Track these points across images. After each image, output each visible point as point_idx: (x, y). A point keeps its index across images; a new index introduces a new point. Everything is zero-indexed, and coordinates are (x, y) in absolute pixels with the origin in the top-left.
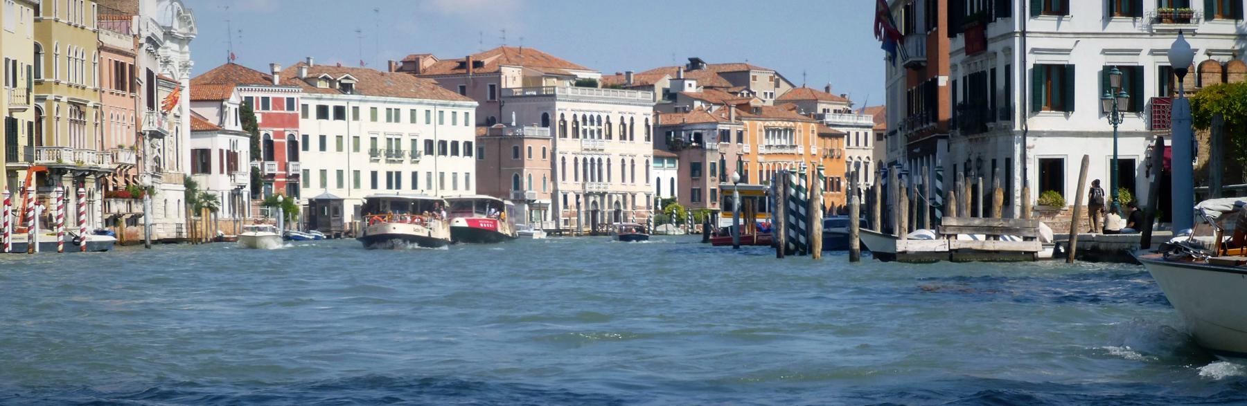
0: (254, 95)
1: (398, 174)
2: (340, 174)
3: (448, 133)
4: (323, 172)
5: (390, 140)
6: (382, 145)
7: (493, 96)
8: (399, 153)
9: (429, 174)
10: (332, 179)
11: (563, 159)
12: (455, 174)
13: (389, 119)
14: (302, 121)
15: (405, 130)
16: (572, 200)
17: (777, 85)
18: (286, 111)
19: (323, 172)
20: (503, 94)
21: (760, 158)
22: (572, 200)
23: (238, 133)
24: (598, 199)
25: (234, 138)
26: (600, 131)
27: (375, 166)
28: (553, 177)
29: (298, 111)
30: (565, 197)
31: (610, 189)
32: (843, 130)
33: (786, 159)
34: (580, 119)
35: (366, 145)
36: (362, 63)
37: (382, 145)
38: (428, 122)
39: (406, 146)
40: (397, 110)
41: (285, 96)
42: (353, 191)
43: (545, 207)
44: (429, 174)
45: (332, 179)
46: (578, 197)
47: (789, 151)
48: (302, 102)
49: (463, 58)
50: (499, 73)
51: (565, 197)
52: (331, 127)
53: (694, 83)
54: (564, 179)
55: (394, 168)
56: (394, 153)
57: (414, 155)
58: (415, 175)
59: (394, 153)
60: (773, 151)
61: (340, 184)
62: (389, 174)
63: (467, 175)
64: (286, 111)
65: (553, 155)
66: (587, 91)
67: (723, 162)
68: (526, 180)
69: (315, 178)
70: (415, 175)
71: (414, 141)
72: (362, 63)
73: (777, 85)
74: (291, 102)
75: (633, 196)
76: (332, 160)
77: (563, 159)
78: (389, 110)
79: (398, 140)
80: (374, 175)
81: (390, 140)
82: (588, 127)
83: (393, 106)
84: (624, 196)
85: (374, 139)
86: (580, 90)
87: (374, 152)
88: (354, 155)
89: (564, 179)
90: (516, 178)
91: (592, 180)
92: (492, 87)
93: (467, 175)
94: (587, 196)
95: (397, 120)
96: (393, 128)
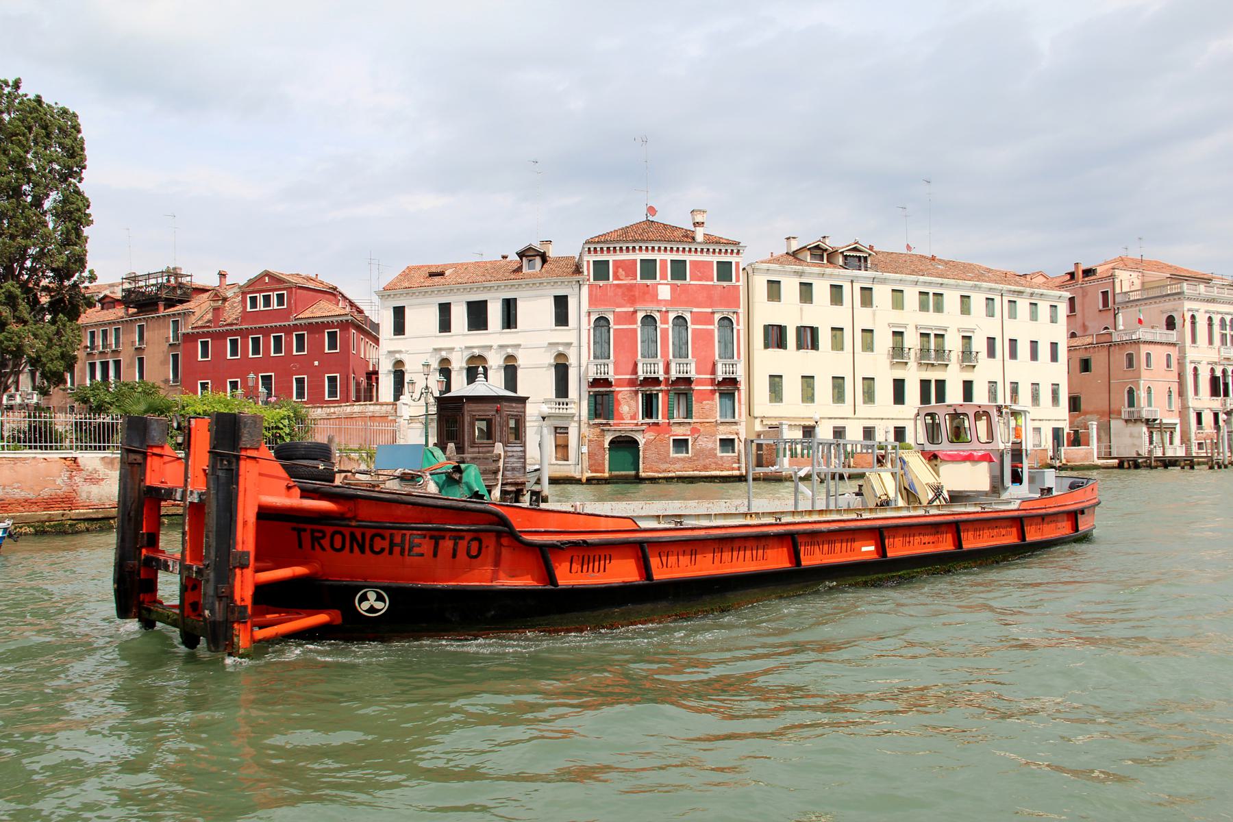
0: (658, 257)
1: (941, 384)
3: (1022, 329)
6: (912, 341)
7: (1105, 303)
8: (940, 352)
11: (1195, 369)
12: (1035, 385)
13: (924, 307)
16: (1208, 419)
20: (1118, 299)
28: (1182, 393)
30: (1199, 415)
35: (884, 341)
36: (908, 247)
37: (912, 341)
39: (953, 344)
46: (1216, 415)
50: (1112, 276)
51: (1199, 415)
54: (1196, 393)
57: (967, 355)
62: (925, 384)
65: (1181, 364)
68: (1143, 394)
71: (967, 339)
72: (908, 247)
77: (1195, 369)
81: (925, 336)
87: (898, 351)
89: (1196, 393)
90: (1131, 392)
92: (1105, 294)
95: (939, 308)
96: (931, 320)
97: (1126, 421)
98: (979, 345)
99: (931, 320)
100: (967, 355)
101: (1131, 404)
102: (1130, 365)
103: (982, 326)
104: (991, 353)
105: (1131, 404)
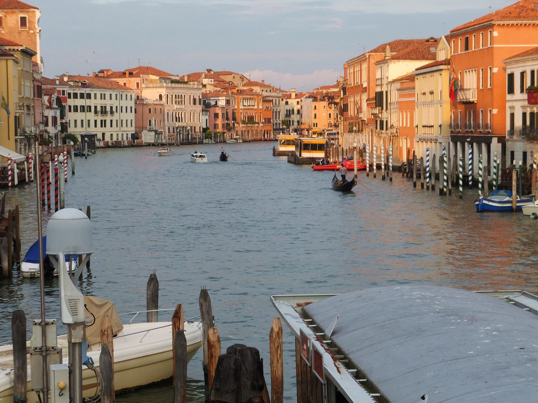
1: (105, 121)
2: (82, 121)
3: (124, 103)
4: (76, 121)
5: (102, 107)
6: (99, 109)
9: (117, 120)
10: (79, 123)
13: (101, 99)
14: (68, 100)
15: (108, 103)
16: (171, 130)
17: (243, 80)
18: (62, 96)
19: (76, 121)
21: (241, 111)
22: (171, 130)
23: (56, 109)
24: (181, 129)
25: (56, 110)
26: (181, 101)
27: (96, 118)
28: (164, 121)
29: (66, 95)
31: (185, 125)
32: (271, 99)
33: (250, 111)
34: (174, 96)
37: (99, 109)
38: (116, 99)
39: (108, 109)
40: (105, 94)
41: (61, 89)
42: (88, 129)
43: (161, 133)
44: (117, 120)
45: (79, 123)
47: (251, 107)
48: (68, 91)
49: (123, 70)
52: (79, 102)
53: (213, 80)
55: (103, 118)
56: (104, 111)
58: (111, 121)
59: (104, 111)
60: (246, 107)
61: (82, 126)
62: (102, 121)
63: (131, 120)
64: (62, 96)
66: (176, 85)
67: (227, 113)
69: (72, 124)
70: (111, 121)
71: (111, 108)
73: (243, 80)
74: (64, 91)
75: (195, 128)
76: (79, 116)
78: (101, 94)
79: (105, 107)
80: (96, 121)
82: (177, 100)
83: (103, 93)
84: (191, 128)
85: (96, 107)
86: (173, 85)
88: (88, 114)
90: (150, 121)
91: (179, 121)
93: (131, 120)
94: (177, 128)
95: (105, 99)
97: (149, 131)
98: (114, 109)
99: (103, 102)
100: (112, 113)
101: (150, 125)
102: (150, 112)
103: (115, 103)
104: (117, 112)
105: (150, 125)
